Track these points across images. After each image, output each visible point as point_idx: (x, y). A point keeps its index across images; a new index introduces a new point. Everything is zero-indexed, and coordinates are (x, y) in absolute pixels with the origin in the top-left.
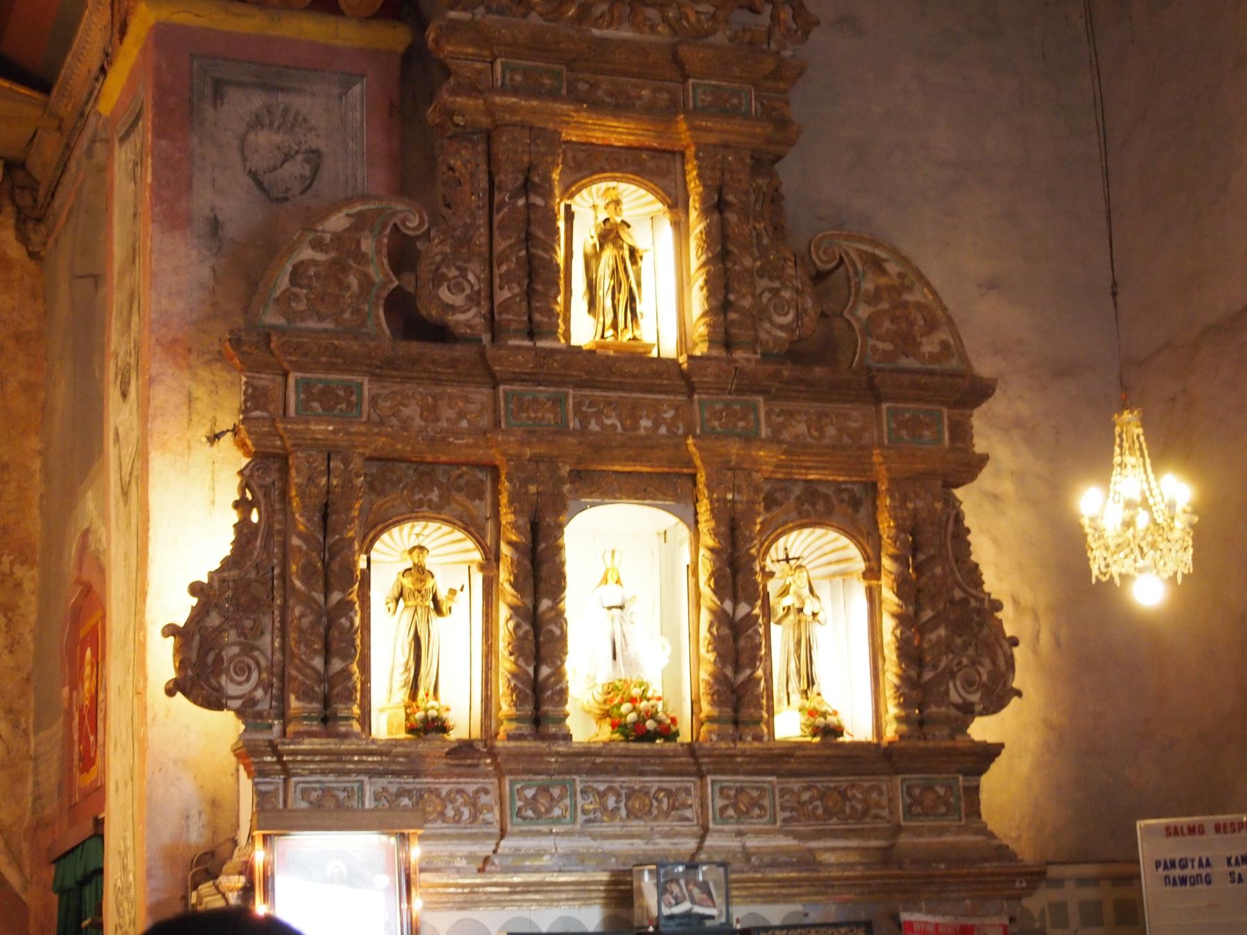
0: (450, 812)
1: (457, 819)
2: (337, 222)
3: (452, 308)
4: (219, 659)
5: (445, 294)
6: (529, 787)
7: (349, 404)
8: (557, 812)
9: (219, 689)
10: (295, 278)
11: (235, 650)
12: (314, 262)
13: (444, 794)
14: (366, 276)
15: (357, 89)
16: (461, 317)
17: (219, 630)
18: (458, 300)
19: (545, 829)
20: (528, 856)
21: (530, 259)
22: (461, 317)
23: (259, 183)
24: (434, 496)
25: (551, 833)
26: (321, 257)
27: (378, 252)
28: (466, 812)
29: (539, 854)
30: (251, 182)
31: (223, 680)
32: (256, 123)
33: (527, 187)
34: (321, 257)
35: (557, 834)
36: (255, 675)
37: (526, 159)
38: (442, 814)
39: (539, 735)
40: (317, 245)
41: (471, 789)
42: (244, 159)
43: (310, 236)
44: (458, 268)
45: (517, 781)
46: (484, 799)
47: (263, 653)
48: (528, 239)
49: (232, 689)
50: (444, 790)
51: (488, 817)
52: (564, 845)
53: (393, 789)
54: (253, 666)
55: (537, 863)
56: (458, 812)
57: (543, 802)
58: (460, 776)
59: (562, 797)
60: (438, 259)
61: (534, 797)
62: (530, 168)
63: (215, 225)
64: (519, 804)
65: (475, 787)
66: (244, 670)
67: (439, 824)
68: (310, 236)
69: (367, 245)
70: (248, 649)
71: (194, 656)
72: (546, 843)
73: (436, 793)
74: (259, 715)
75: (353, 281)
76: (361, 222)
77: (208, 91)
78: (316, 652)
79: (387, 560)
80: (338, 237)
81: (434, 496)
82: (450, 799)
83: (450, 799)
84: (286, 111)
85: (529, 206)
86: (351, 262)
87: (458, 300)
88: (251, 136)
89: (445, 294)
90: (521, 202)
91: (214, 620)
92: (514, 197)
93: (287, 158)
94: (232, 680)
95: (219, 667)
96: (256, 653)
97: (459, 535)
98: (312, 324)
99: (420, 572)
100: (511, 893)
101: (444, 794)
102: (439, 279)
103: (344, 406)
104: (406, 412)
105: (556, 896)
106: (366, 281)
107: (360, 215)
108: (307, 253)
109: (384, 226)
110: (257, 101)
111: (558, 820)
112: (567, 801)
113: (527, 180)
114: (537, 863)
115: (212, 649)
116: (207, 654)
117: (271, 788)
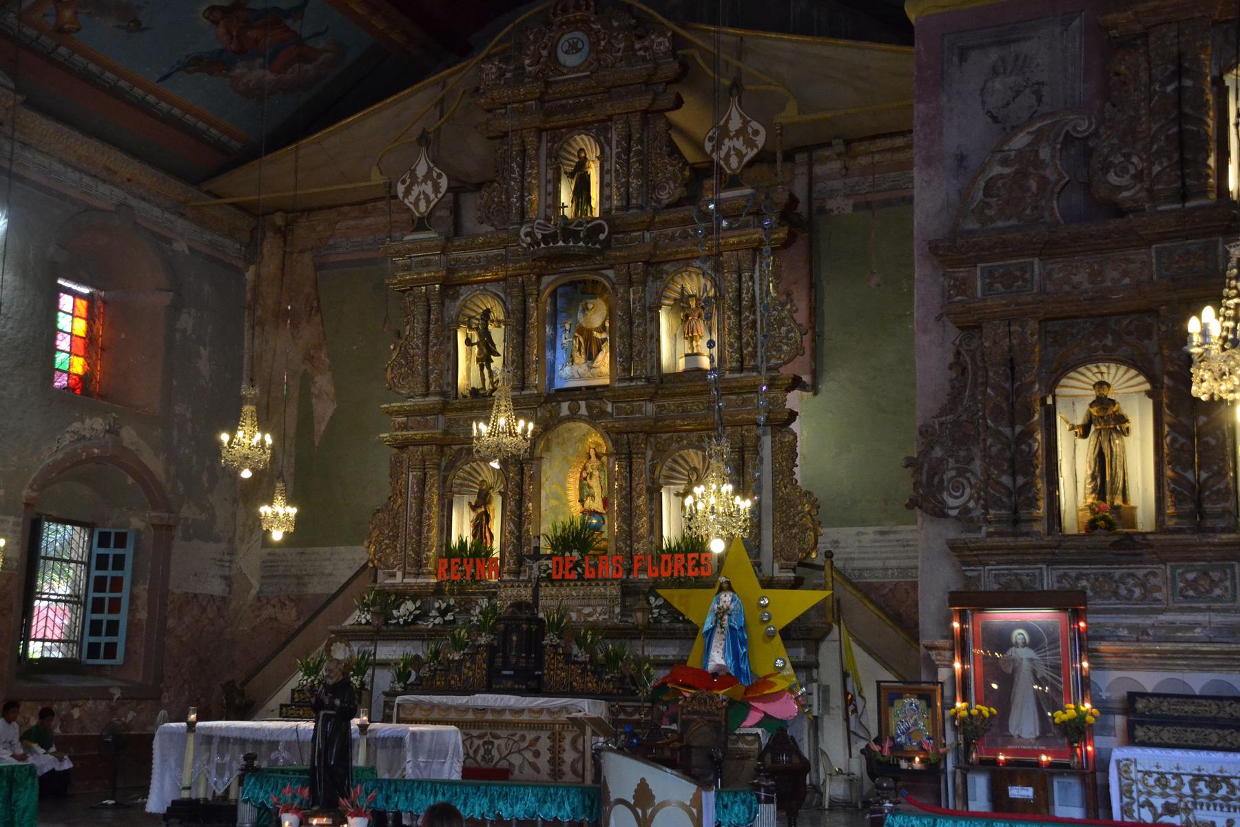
0: (1123, 592)
1: (1128, 599)
2: (1020, 141)
3: (1120, 188)
4: (941, 481)
5: (1112, 178)
6: (1191, 571)
7: (1024, 280)
8: (1217, 592)
9: (943, 502)
10: (987, 192)
11: (953, 473)
12: (1001, 176)
13: (1117, 577)
14: (1044, 178)
15: (1077, 22)
16: (1126, 194)
17: (941, 460)
18: (1125, 181)
19: (1202, 605)
20: (1179, 629)
21: (1181, 132)
22: (1126, 194)
23: (995, 119)
24: (1109, 341)
25: (1209, 609)
26: (1007, 171)
27: (1053, 157)
28: (1138, 592)
29: (1192, 626)
30: (989, 120)
31: (945, 495)
32: (995, 72)
33: (1180, 73)
34: (1007, 171)
35: (1214, 610)
36: (968, 491)
37: (1175, 50)
38: (1115, 593)
39: (1200, 529)
40: (1005, 162)
41: (1141, 573)
42: (983, 103)
43: (998, 156)
44: (1124, 155)
45: (1178, 567)
46: (1153, 581)
47: (973, 473)
48: (1181, 118)
49: (951, 502)
50: (1117, 574)
51: (1157, 595)
52: (1218, 619)
53: (1073, 574)
54: (965, 482)
55: (1189, 634)
56: (1131, 591)
57: (1204, 583)
58: (1128, 563)
59: (1221, 580)
60: (1106, 151)
61: (1195, 580)
62: (1180, 56)
63: (961, 159)
64: (1182, 585)
65: (1145, 571)
66: (959, 487)
67: (1113, 600)
68: (998, 156)
69: (1044, 154)
70: (961, 472)
71: (924, 478)
72: (1200, 618)
73: (1109, 577)
74: (972, 520)
75: (1033, 184)
76: (1039, 136)
77: (955, 59)
78: (1004, 472)
79: (1074, 399)
80: (1019, 151)
81: (1109, 341)
82: (1122, 580)
83: (1122, 580)
84: (1017, 58)
85: (1180, 89)
86: (1031, 169)
87: (1125, 181)
88: (989, 85)
89: (1112, 178)
90: (1170, 88)
91: (938, 452)
92: (1164, 85)
93: (1018, 93)
94: (951, 496)
95: (941, 487)
96: (968, 475)
97: (1133, 372)
98: (1000, 224)
99: (1103, 402)
100: (1161, 658)
101: (1117, 577)
102: (1106, 168)
103: (1020, 283)
104: (1075, 279)
105: (1203, 663)
106: (1043, 181)
107: (1040, 130)
108: (997, 170)
109: (1058, 135)
110: (994, 55)
111: (1219, 599)
112: (1228, 583)
113: (1180, 66)
114: (1189, 634)
115: (936, 473)
116: (933, 478)
117: (975, 573)
